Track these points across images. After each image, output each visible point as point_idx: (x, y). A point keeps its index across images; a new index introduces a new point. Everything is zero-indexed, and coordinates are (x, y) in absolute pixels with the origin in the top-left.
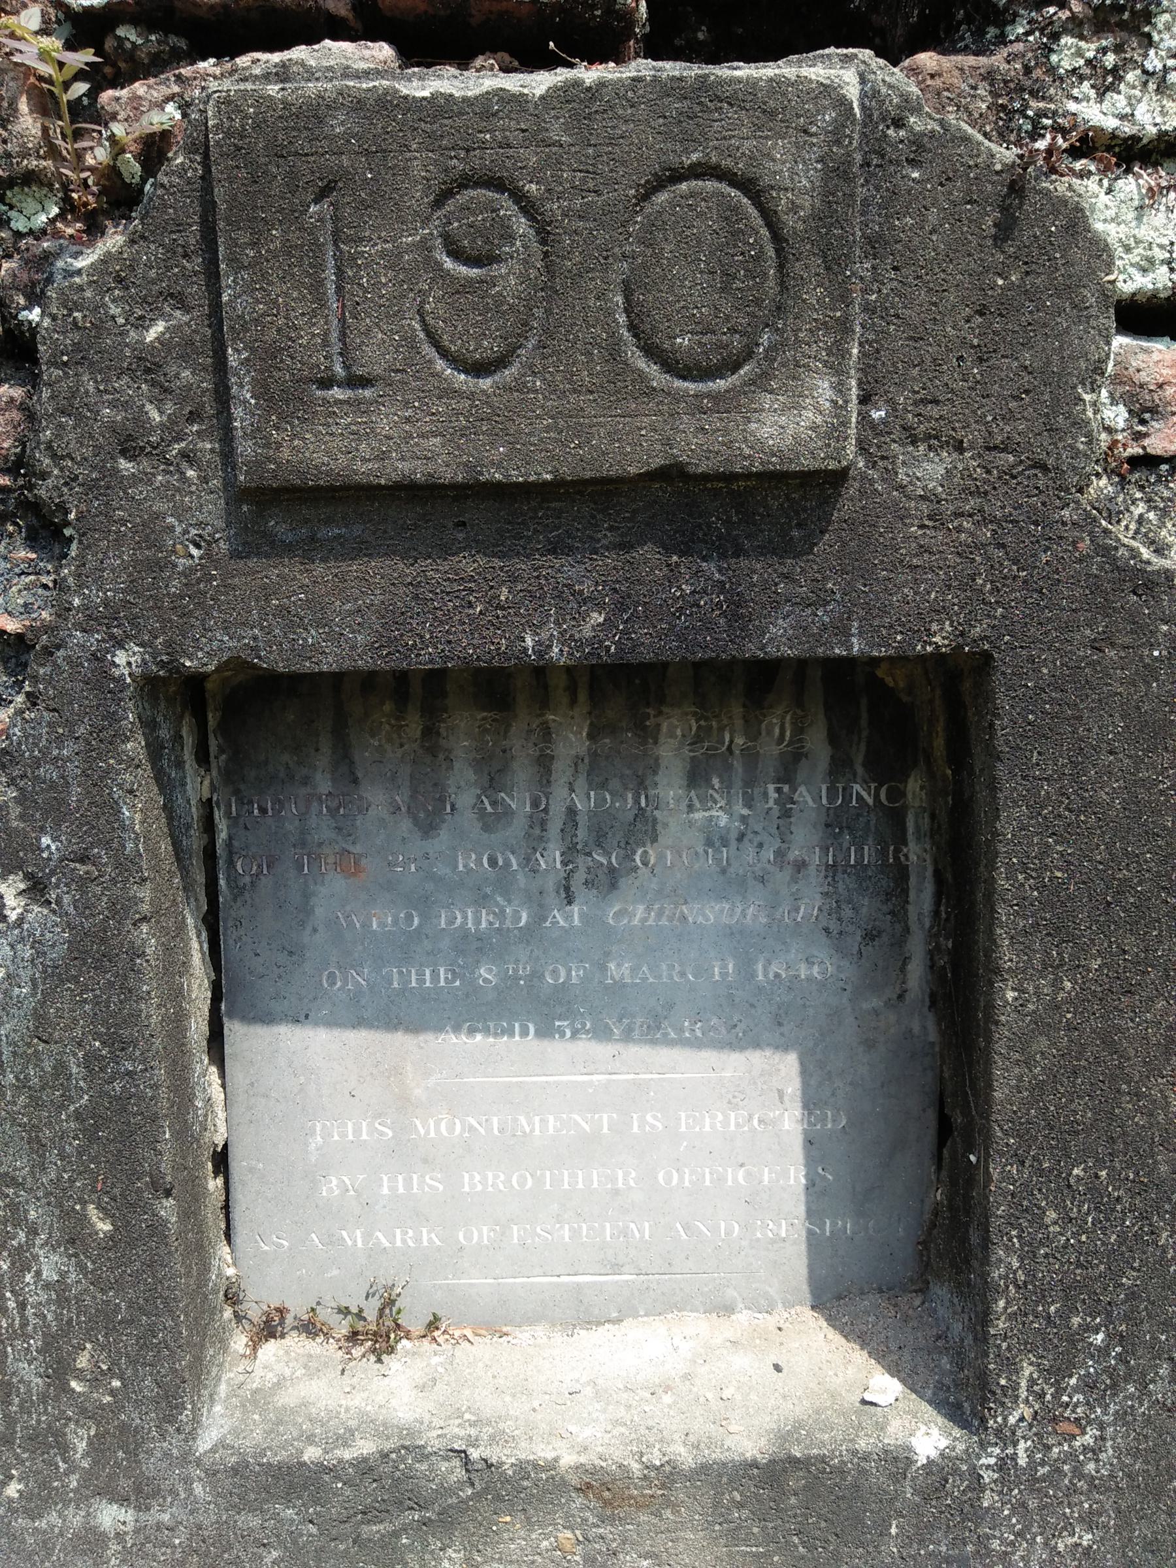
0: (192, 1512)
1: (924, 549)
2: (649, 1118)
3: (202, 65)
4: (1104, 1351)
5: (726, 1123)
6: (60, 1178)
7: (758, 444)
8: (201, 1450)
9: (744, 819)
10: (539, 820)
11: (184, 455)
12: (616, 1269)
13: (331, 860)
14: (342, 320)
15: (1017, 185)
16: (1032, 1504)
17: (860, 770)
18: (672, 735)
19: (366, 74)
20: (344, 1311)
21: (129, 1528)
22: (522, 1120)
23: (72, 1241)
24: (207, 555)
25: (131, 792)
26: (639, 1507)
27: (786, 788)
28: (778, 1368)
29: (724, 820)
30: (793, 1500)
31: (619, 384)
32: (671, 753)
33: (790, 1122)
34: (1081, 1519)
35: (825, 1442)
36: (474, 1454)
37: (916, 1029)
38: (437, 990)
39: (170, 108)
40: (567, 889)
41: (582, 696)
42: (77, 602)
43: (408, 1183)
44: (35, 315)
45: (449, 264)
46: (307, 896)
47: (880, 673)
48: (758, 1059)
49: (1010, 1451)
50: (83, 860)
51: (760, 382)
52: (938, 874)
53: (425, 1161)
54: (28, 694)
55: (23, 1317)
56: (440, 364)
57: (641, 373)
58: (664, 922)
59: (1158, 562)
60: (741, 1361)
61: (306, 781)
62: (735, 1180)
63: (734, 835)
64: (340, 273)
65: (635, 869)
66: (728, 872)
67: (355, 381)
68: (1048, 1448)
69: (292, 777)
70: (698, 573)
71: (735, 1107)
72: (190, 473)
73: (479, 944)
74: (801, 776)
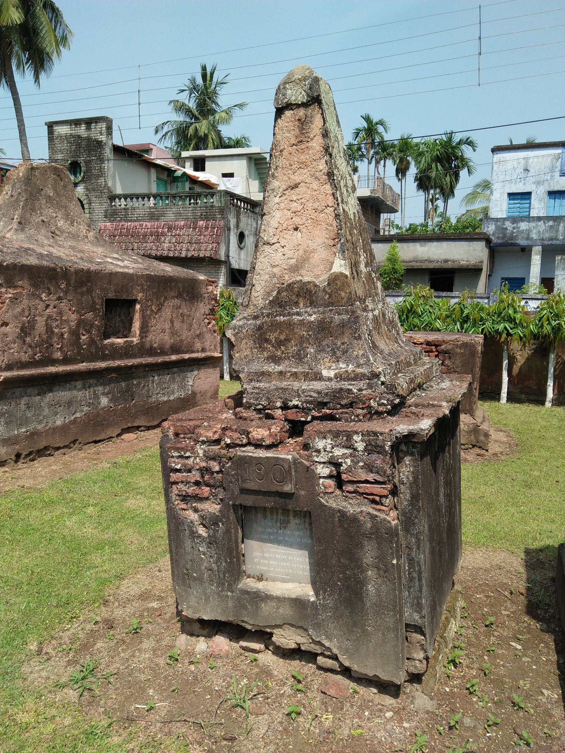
15: (308, 467)
33: (307, 560)
35: (302, 598)
48: (303, 551)
51: (285, 484)
60: (299, 589)
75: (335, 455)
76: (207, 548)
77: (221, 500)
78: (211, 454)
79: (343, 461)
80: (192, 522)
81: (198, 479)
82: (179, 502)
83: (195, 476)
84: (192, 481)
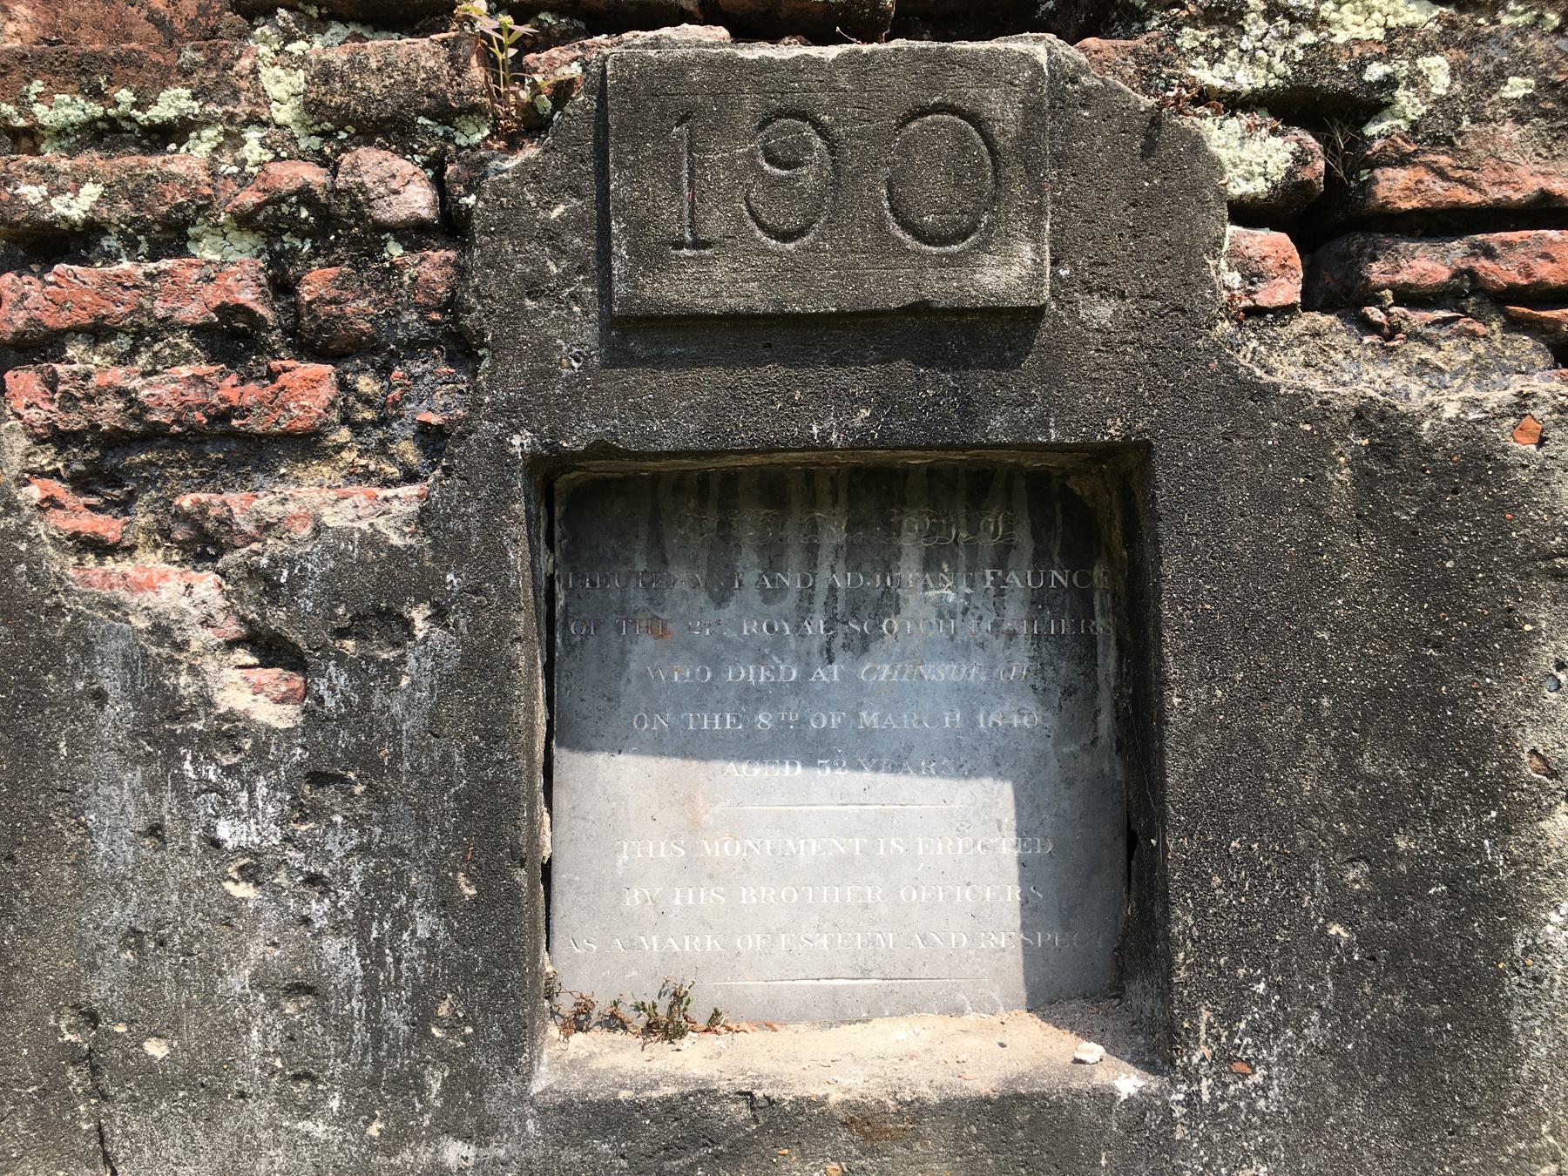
0: (524, 1148)
1: (1100, 367)
2: (893, 842)
3: (596, 39)
4: (1265, 999)
5: (955, 848)
6: (438, 849)
7: (981, 288)
8: (534, 1091)
9: (967, 597)
10: (807, 596)
11: (572, 296)
12: (865, 974)
13: (643, 624)
14: (692, 203)
15: (1156, 120)
16: (1216, 1137)
17: (1057, 559)
18: (911, 530)
19: (713, 45)
20: (640, 1007)
21: (470, 1163)
22: (790, 843)
23: (443, 904)
24: (584, 367)
25: (516, 541)
26: (894, 1140)
27: (1000, 573)
28: (1002, 1045)
29: (951, 597)
30: (1020, 1134)
31: (884, 246)
32: (911, 545)
33: (1007, 848)
34: (1257, 1153)
36: (759, 1094)
37: (1107, 770)
38: (725, 732)
39: (575, 65)
40: (829, 651)
41: (842, 498)
42: (487, 399)
43: (696, 894)
44: (471, 200)
45: (767, 167)
46: (624, 652)
47: (1070, 484)
49: (1195, 1087)
50: (475, 593)
51: (983, 246)
52: (1119, 642)
53: (711, 876)
54: (444, 468)
55: (398, 970)
56: (759, 233)
57: (899, 240)
58: (905, 679)
59: (1267, 378)
60: (971, 1042)
61: (627, 561)
62: (963, 896)
63: (959, 610)
64: (692, 172)
65: (882, 636)
66: (955, 640)
67: (698, 244)
68: (1226, 1086)
69: (616, 557)
70: (938, 382)
71: (962, 835)
72: (576, 309)
73: (757, 695)
74: (1011, 563)
75: (1341, 38)
76: (282, 820)
77: (432, 439)
78: (375, 86)
79: (1401, 67)
80: (161, 631)
81: (246, 296)
82: (58, 488)
83: (226, 270)
84: (192, 312)
